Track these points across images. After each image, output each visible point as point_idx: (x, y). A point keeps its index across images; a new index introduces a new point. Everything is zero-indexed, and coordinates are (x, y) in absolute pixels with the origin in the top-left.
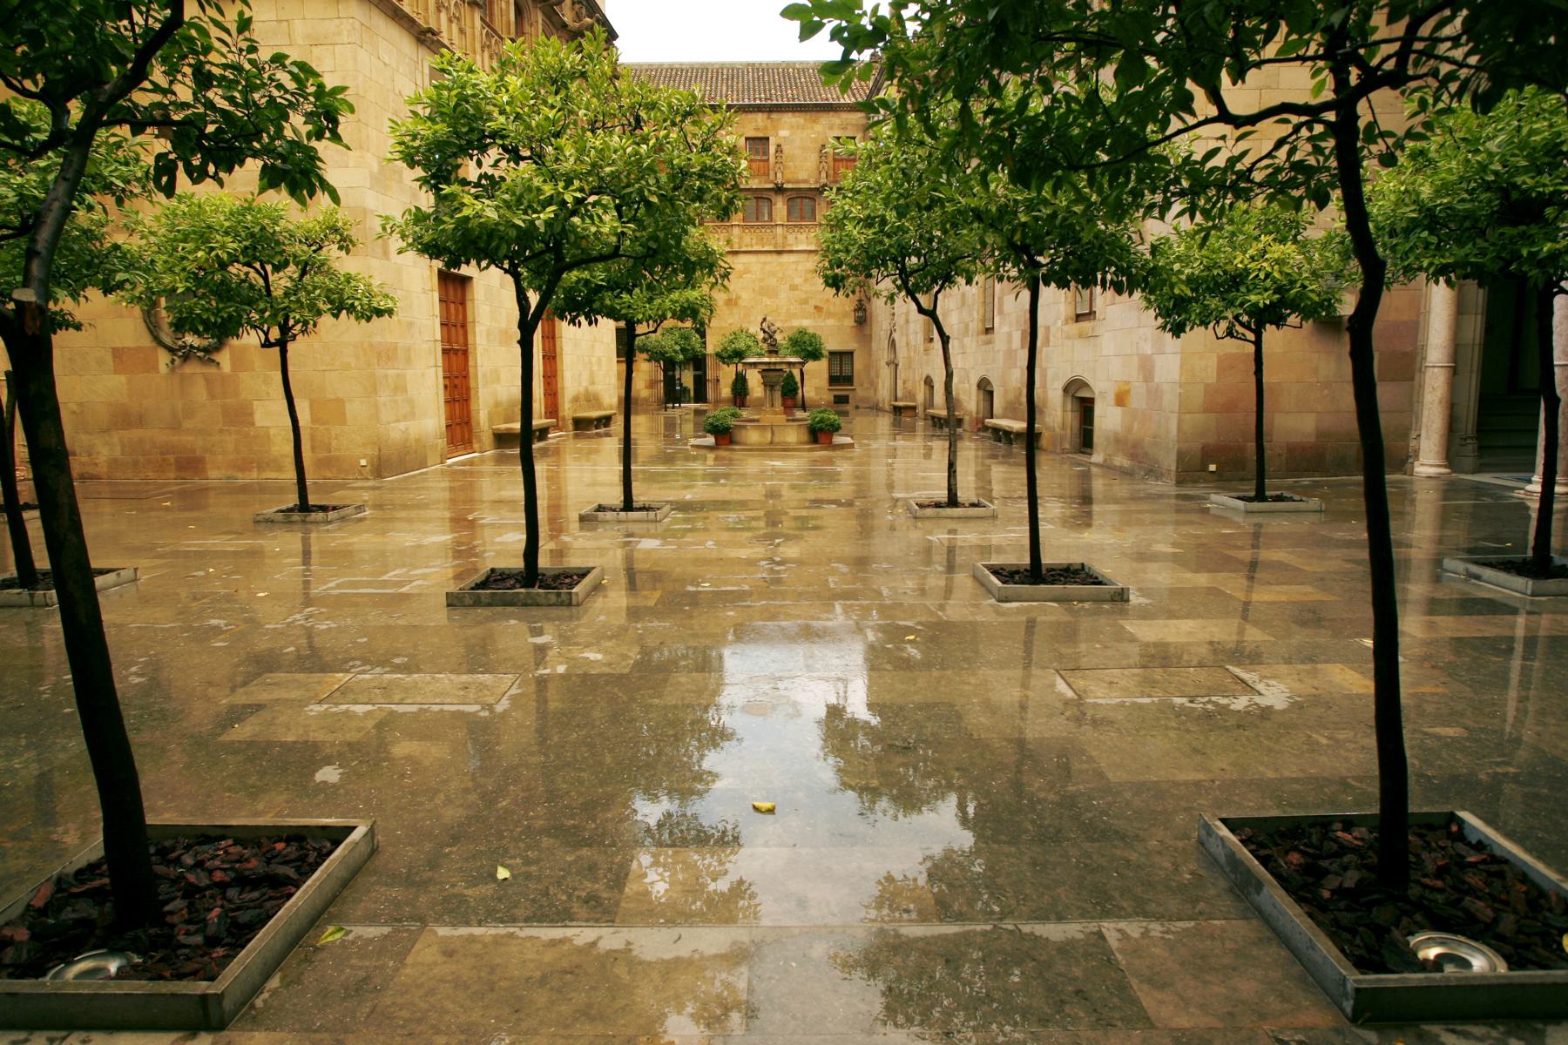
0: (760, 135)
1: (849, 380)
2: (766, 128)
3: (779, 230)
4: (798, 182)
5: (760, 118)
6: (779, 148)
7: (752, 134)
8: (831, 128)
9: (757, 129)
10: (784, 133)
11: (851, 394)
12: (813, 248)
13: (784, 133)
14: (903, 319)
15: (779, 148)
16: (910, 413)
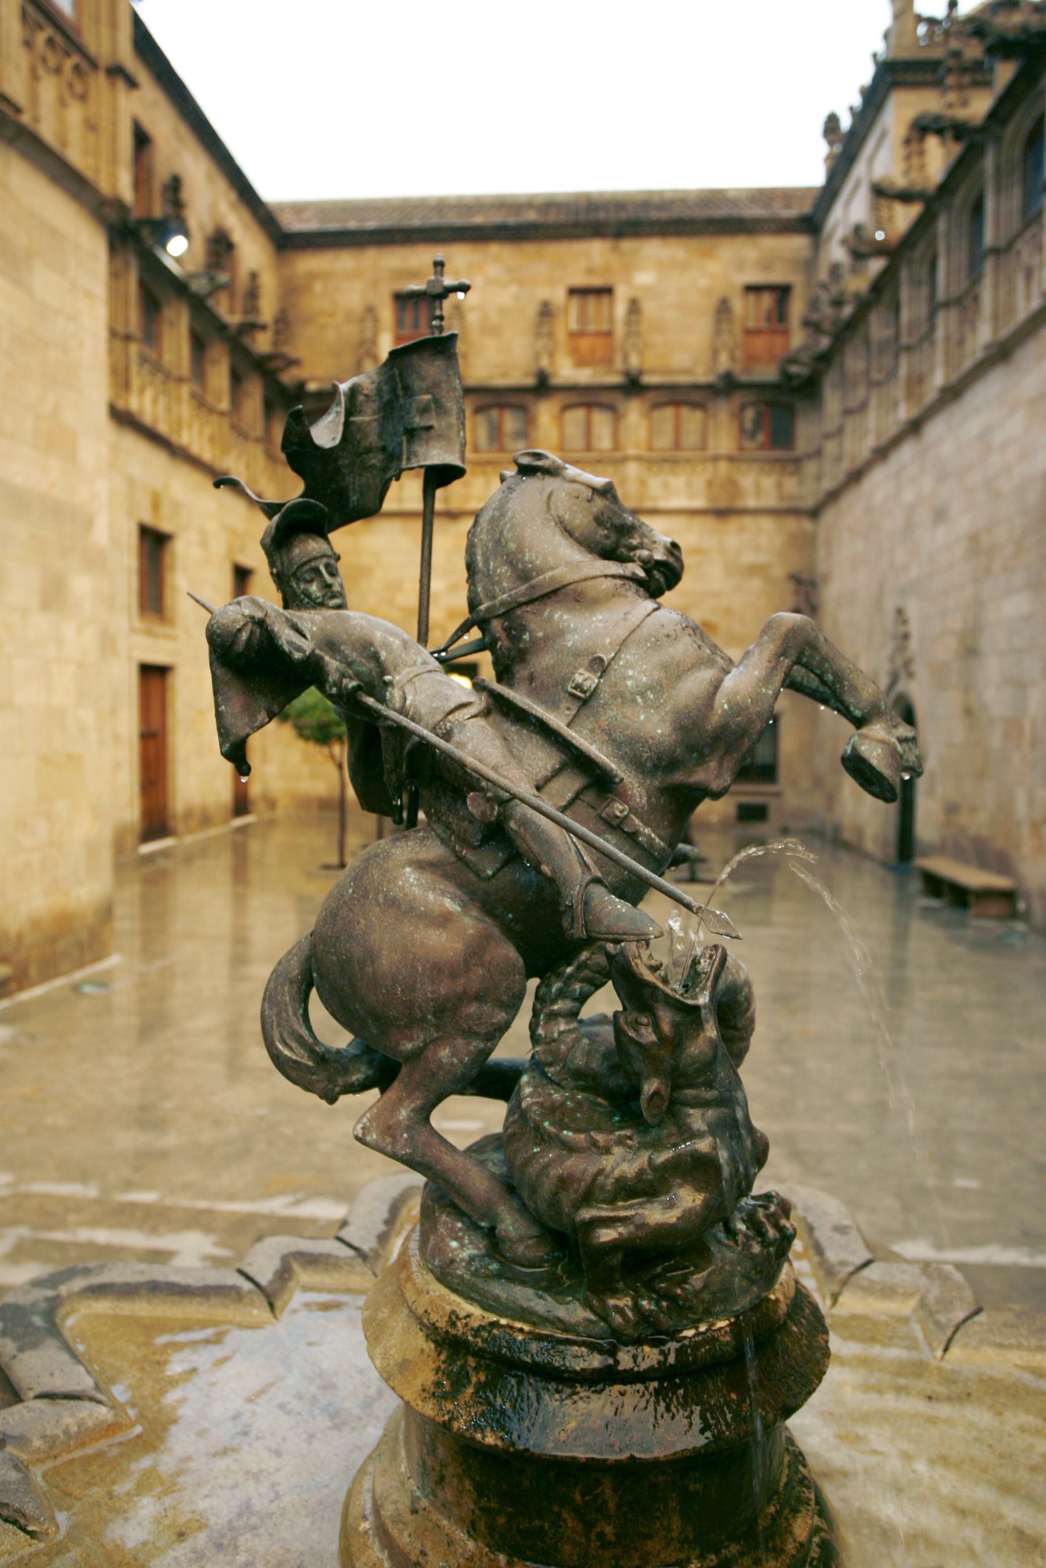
0: (596, 281)
1: (767, 772)
2: (607, 270)
3: (632, 469)
4: (669, 371)
5: (597, 250)
6: (634, 307)
7: (580, 280)
8: (740, 266)
9: (590, 271)
10: (644, 278)
11: (772, 803)
12: (699, 503)
13: (644, 278)
14: (946, 650)
15: (634, 307)
16: (996, 907)
